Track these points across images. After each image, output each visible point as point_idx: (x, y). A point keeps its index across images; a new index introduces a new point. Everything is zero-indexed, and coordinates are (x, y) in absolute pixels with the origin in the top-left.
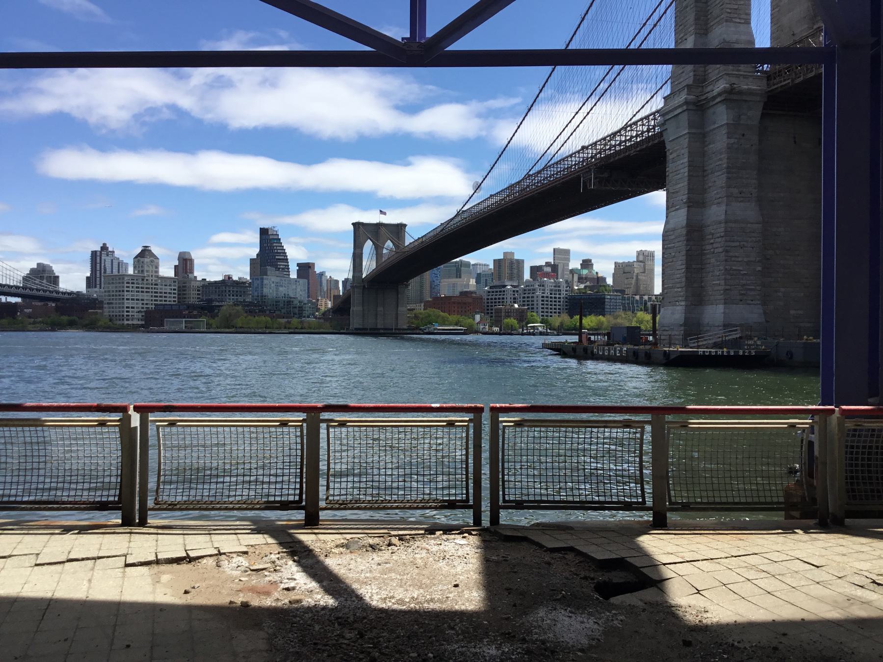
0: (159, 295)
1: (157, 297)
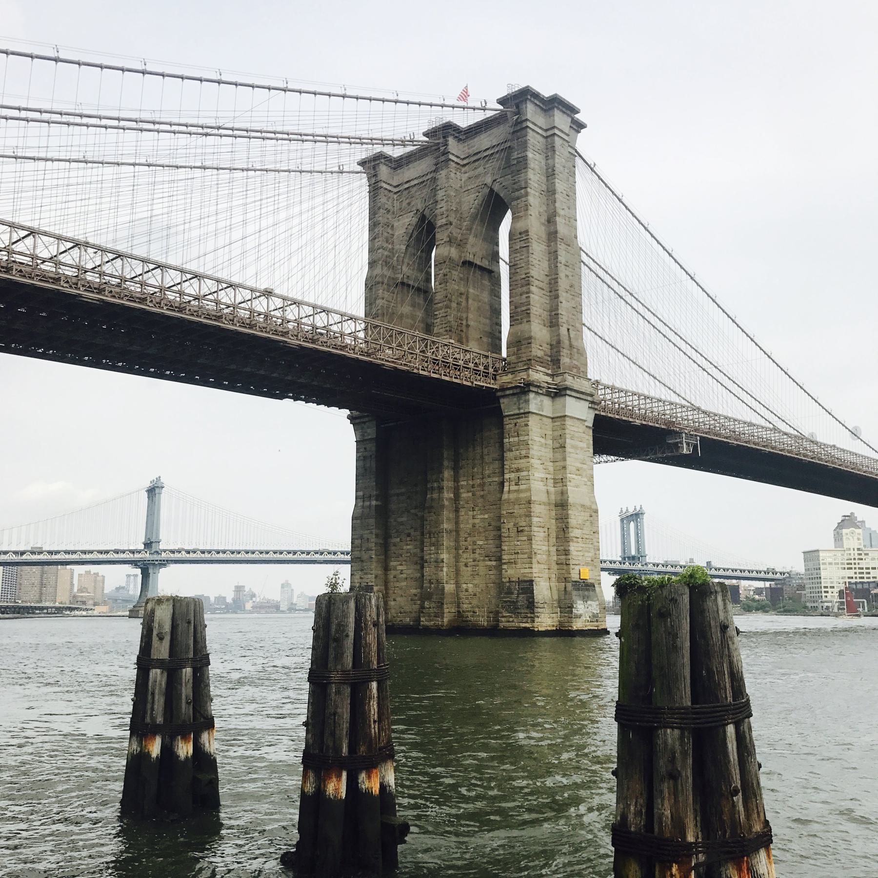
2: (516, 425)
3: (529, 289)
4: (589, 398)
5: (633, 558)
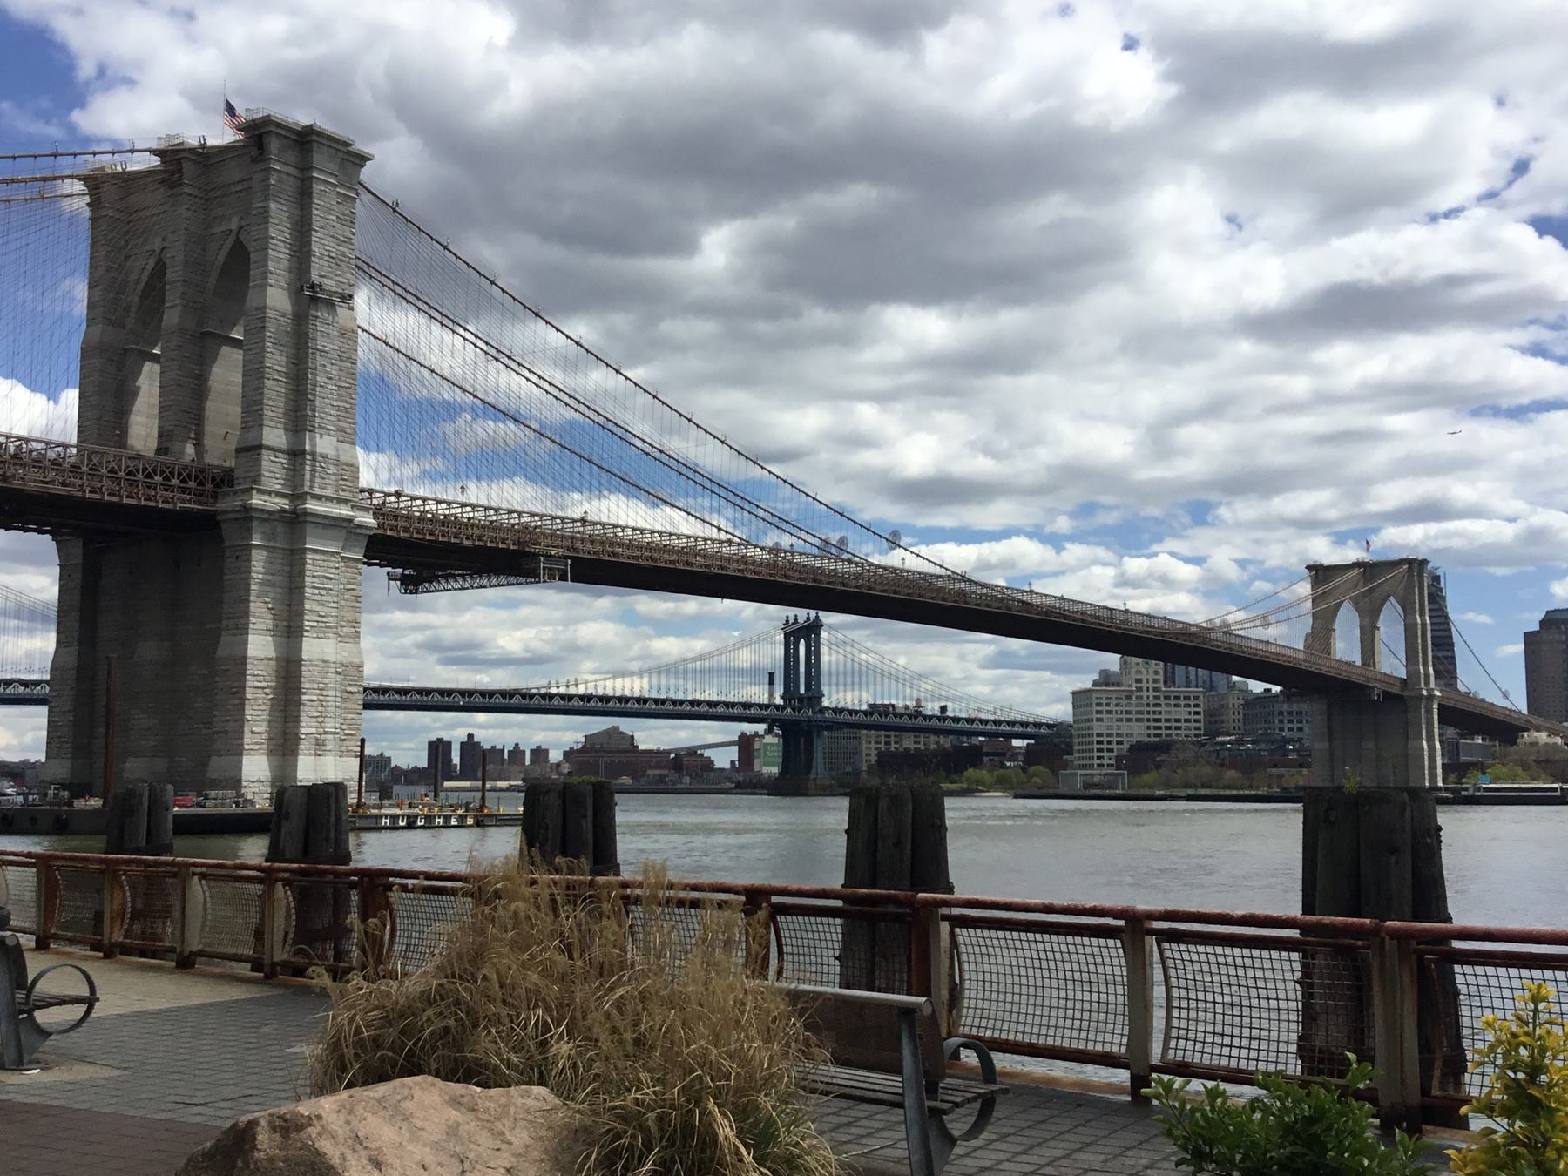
0: (1163, 724)
1: (1160, 728)
2: (237, 558)
3: (263, 383)
4: (344, 524)
5: (801, 699)
